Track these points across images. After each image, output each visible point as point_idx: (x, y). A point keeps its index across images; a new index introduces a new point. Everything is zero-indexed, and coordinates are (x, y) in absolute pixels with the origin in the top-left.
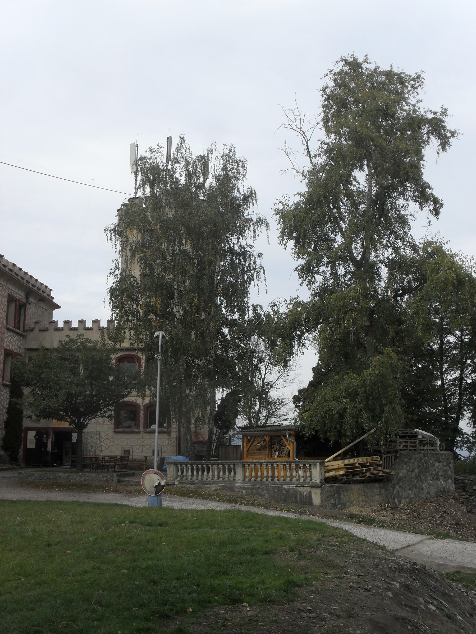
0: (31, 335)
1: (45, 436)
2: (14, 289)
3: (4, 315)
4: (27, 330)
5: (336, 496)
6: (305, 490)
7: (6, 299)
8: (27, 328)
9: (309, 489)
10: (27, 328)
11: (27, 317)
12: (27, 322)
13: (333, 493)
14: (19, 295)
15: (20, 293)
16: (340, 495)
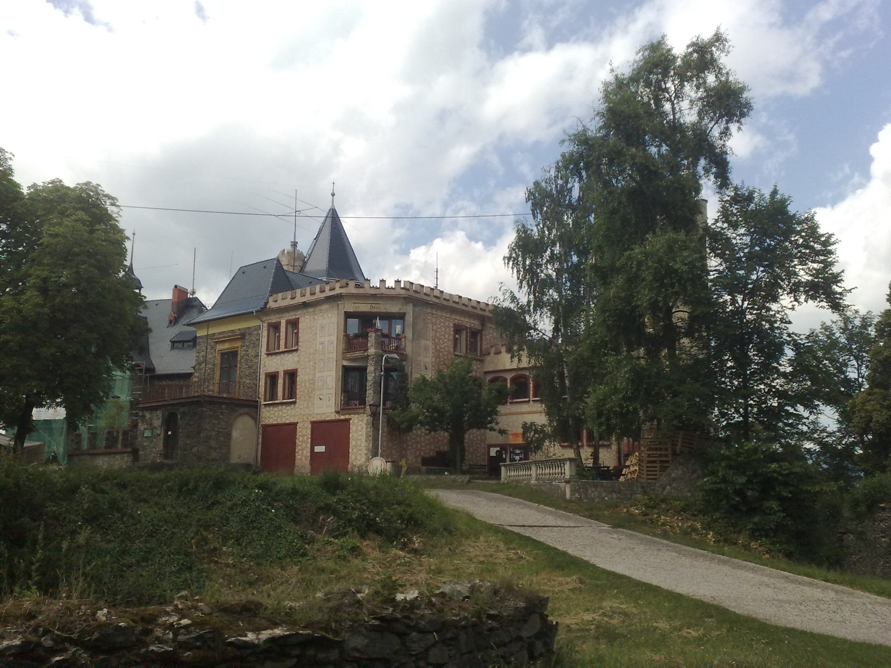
0: (488, 359)
1: (504, 452)
2: (462, 319)
3: (450, 344)
4: (484, 355)
5: (581, 490)
6: (562, 485)
7: (453, 329)
8: (484, 352)
9: (564, 484)
10: (484, 352)
11: (484, 342)
12: (484, 347)
13: (577, 488)
14: (475, 324)
15: (472, 321)
16: (587, 490)
